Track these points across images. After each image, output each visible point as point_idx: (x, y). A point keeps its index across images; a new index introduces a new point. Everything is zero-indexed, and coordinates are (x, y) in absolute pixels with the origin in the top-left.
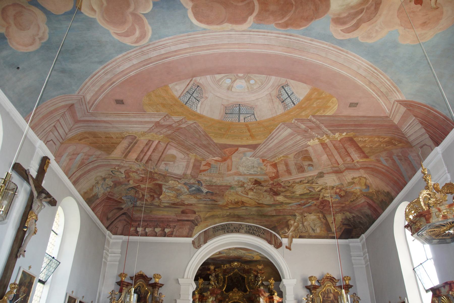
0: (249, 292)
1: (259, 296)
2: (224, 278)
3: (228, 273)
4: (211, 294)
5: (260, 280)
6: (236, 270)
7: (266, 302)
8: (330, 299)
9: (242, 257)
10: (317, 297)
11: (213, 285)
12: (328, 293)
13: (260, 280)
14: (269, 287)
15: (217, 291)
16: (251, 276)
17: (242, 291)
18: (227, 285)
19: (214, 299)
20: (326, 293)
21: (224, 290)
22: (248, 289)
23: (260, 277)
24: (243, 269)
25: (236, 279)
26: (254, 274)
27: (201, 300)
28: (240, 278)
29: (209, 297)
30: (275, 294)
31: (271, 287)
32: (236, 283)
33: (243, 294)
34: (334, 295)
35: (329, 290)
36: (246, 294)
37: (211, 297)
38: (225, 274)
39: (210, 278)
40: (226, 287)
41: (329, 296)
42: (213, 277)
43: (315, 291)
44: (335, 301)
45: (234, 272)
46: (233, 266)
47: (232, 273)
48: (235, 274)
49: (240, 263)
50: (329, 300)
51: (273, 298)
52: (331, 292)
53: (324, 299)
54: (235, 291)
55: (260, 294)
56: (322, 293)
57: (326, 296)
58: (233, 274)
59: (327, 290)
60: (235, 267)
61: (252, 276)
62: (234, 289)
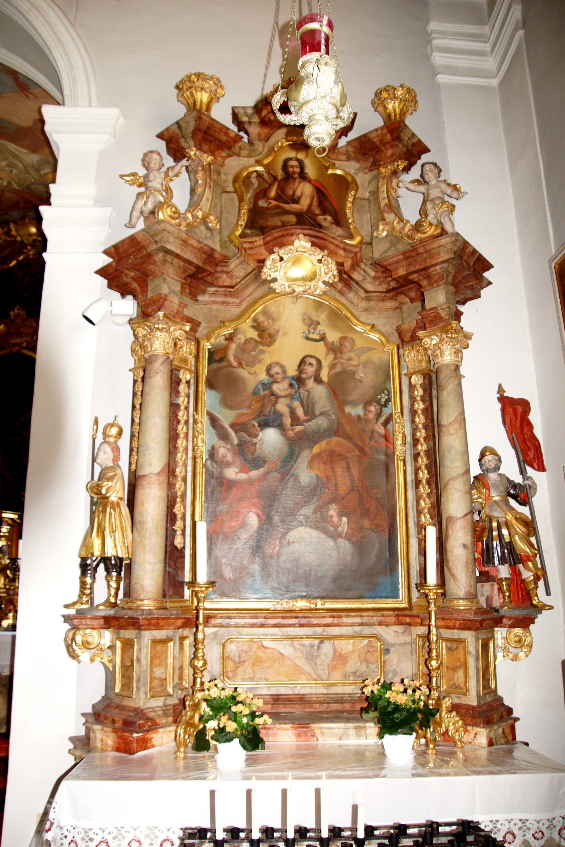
8: (295, 207)
10: (224, 195)
12: (288, 176)
20: (275, 178)
34: (320, 191)
35: (294, 163)
41: (290, 192)
43: (213, 154)
44: (320, 218)
47: (14, 263)
50: (287, 212)
52: (303, 176)
53: (262, 203)
56: (255, 174)
57: (273, 193)
59: (286, 161)
60: (26, 241)
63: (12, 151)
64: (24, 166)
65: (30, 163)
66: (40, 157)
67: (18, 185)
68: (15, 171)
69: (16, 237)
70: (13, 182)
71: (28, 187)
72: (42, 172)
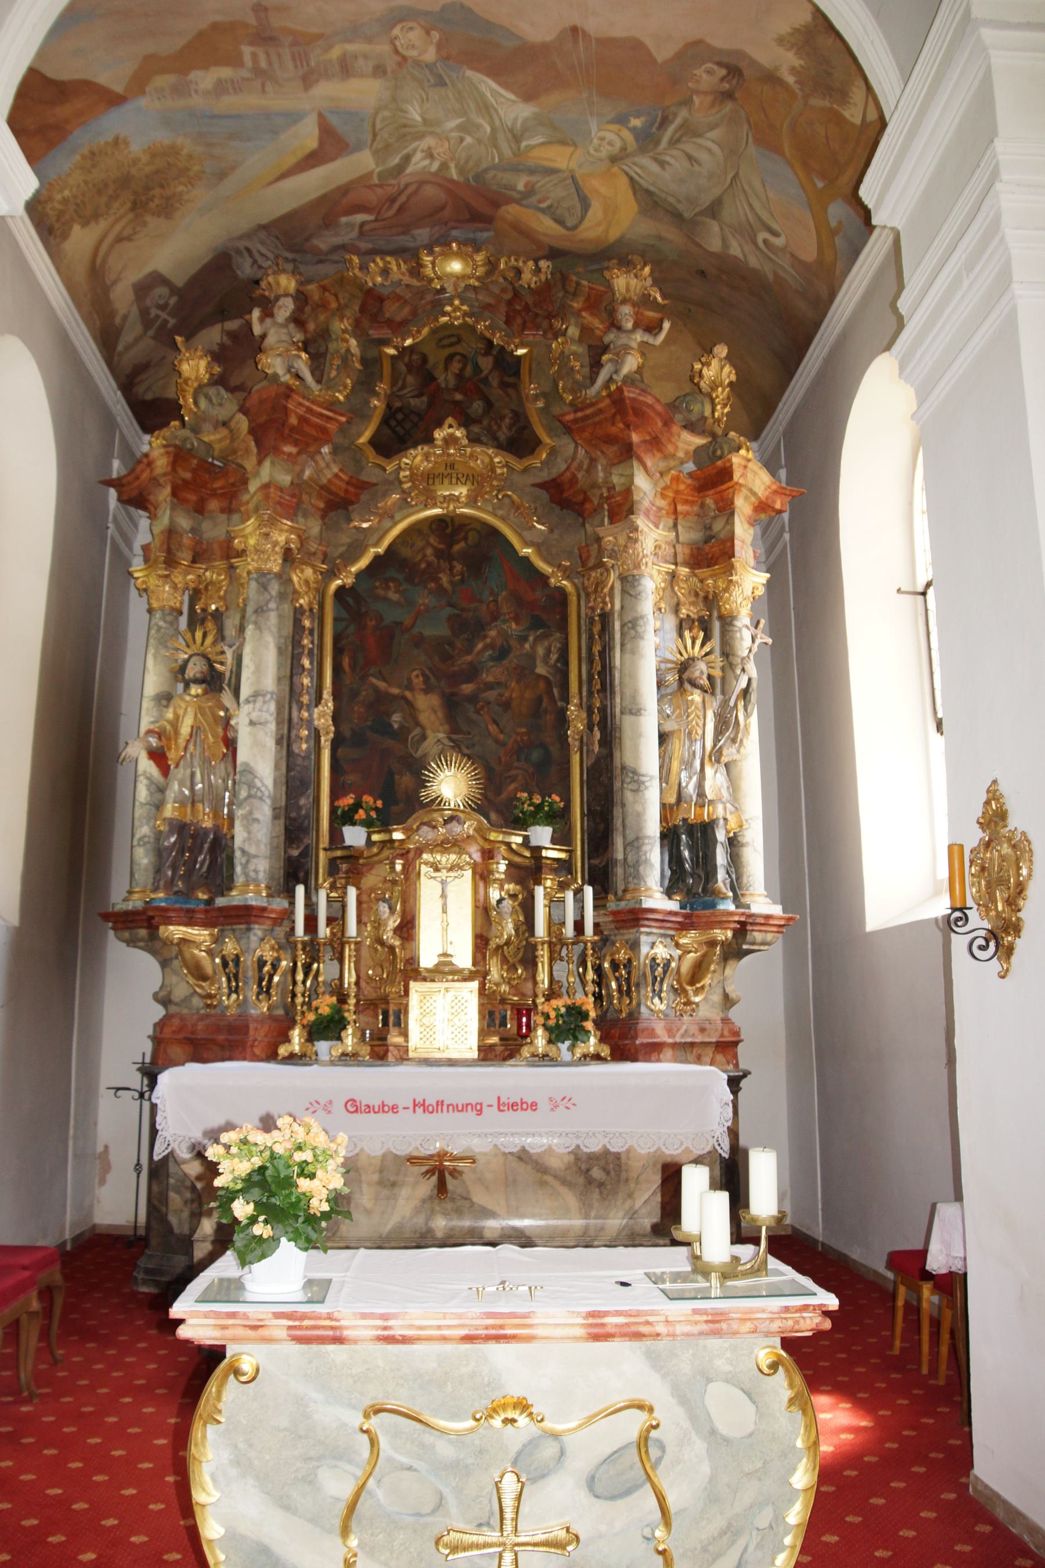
0: (553, 452)
1: (627, 453)
2: (371, 366)
3: (400, 327)
4: (257, 432)
5: (634, 345)
6: (454, 314)
7: (675, 512)
9: (497, 200)
11: (276, 376)
13: (634, 345)
14: (696, 408)
15: (302, 420)
16: (564, 333)
17: (499, 446)
18: (389, 406)
19: (285, 479)
21: (363, 440)
22: (546, 439)
23: (636, 326)
24: (509, 296)
25: (456, 366)
26: (586, 331)
27: (193, 497)
28: (486, 363)
29: (249, 463)
30: (743, 452)
31: (707, 412)
32: (458, 397)
33: (507, 465)
36: (527, 462)
37: (260, 462)
38: (374, 334)
39: (257, 330)
40: (385, 421)
42: (275, 323)
45: (444, 319)
46: (439, 278)
48: (449, 336)
49: (480, 258)
51: (725, 474)
54: (450, 441)
55: (635, 438)
58: (433, 332)
61: (573, 331)
62: (439, 424)
63: (482, 96)
64: (494, 130)
65: (509, 124)
66: (536, 110)
67: (461, 171)
68: (469, 140)
69: (431, 280)
70: (452, 165)
71: (478, 177)
72: (523, 144)
